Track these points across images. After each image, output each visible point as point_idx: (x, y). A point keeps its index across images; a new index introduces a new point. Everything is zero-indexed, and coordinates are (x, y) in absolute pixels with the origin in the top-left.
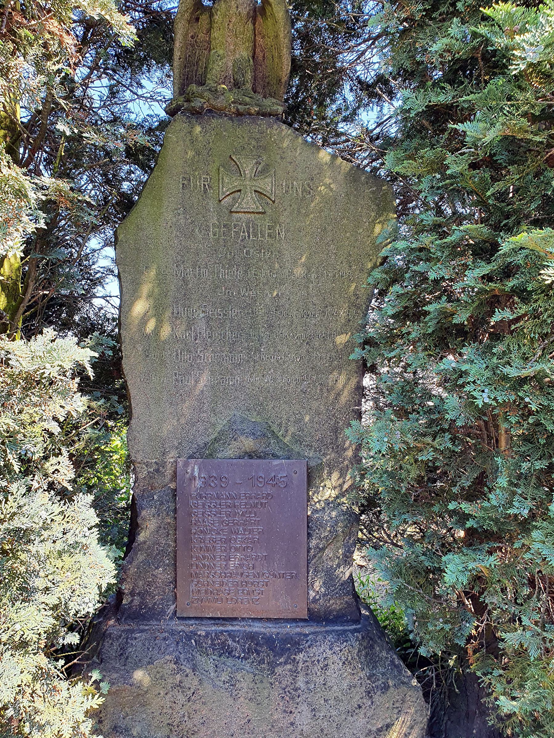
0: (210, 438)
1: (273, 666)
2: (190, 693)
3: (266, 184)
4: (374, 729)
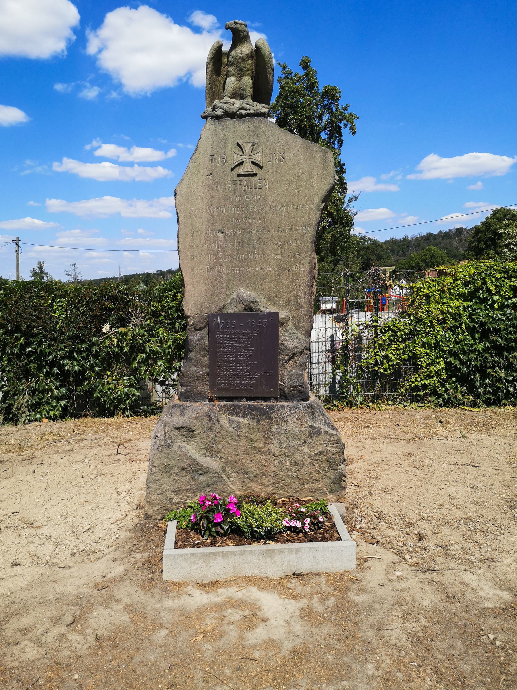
1: (259, 421)
2: (216, 433)
3: (258, 158)
4: (313, 454)
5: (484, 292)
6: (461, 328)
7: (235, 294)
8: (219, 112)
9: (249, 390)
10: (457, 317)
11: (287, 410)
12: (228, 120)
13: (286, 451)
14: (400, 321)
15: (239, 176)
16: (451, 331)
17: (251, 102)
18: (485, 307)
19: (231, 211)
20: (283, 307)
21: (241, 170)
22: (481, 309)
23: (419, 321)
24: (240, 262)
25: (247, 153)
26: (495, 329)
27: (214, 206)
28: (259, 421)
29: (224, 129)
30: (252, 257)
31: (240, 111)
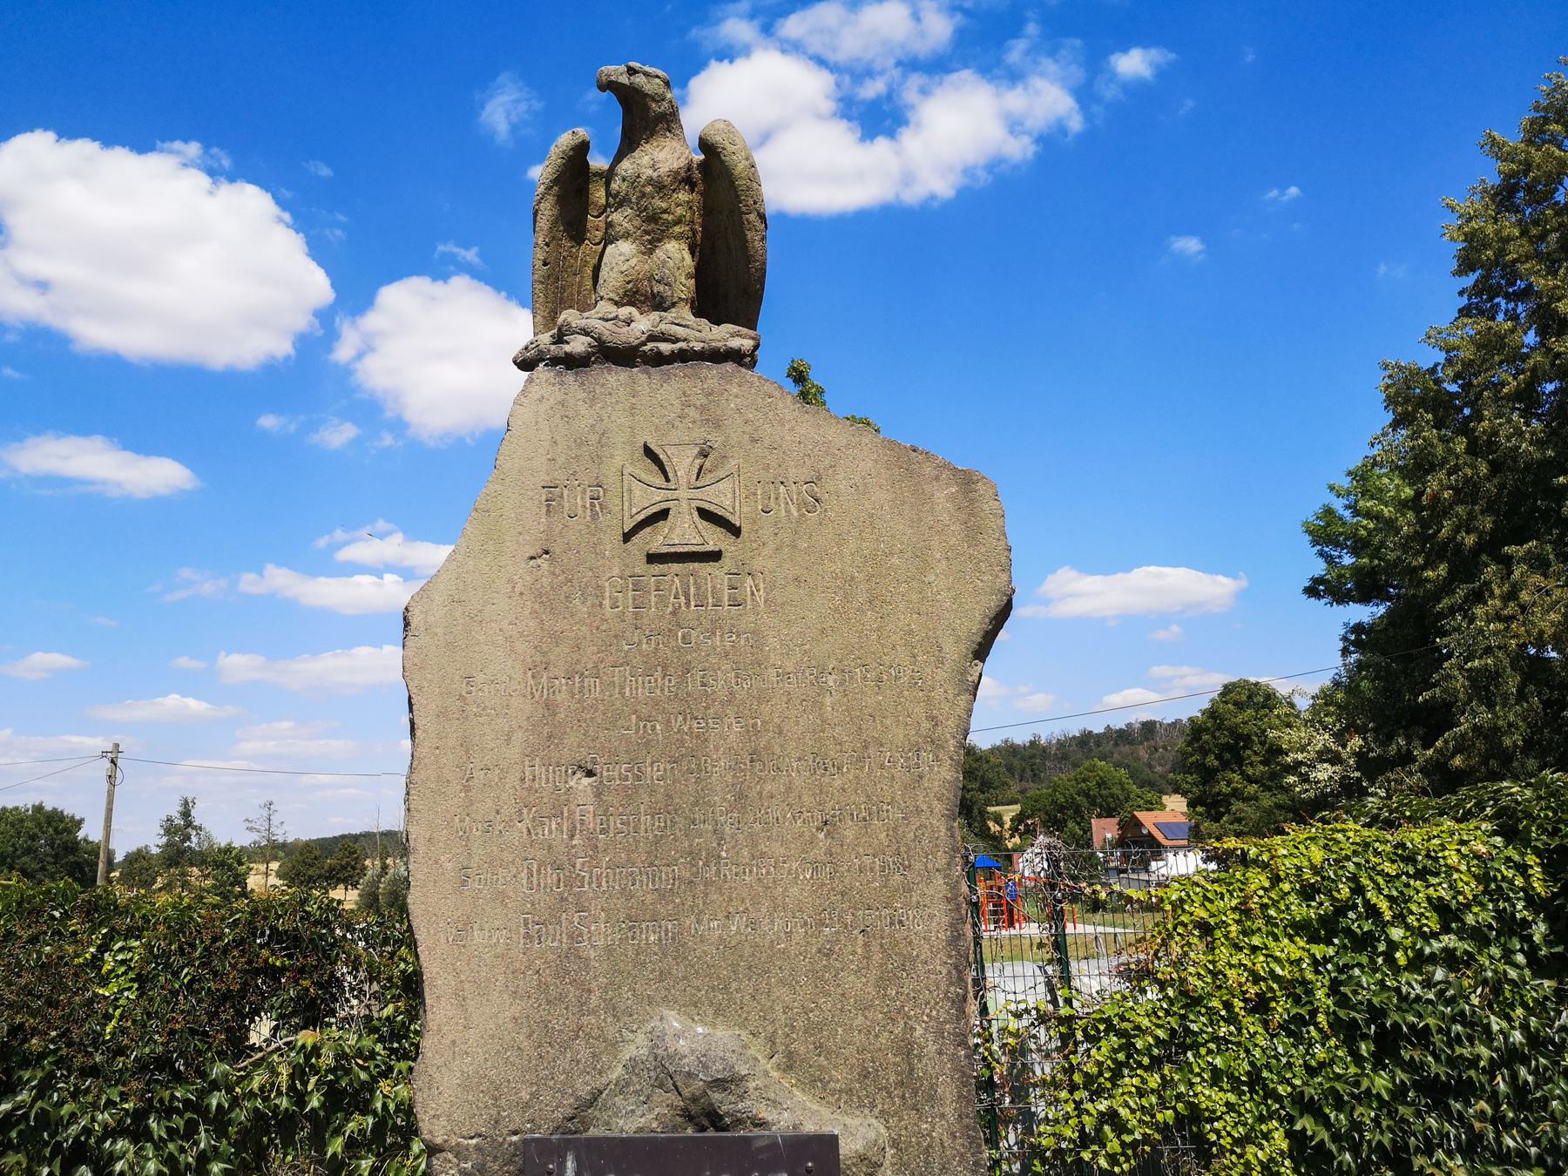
0: (604, 1080)
3: (721, 498)
5: (1359, 917)
6: (1316, 1025)
7: (641, 1039)
8: (578, 345)
10: (1298, 990)
12: (610, 370)
14: (1136, 1002)
15: (653, 558)
16: (1290, 1034)
17: (690, 318)
18: (1372, 961)
19: (622, 688)
20: (847, 1098)
21: (656, 539)
22: (1359, 965)
23: (1193, 1001)
24: (662, 895)
25: (683, 482)
26: (1412, 1027)
27: (554, 672)
29: (593, 401)
30: (710, 873)
31: (650, 345)
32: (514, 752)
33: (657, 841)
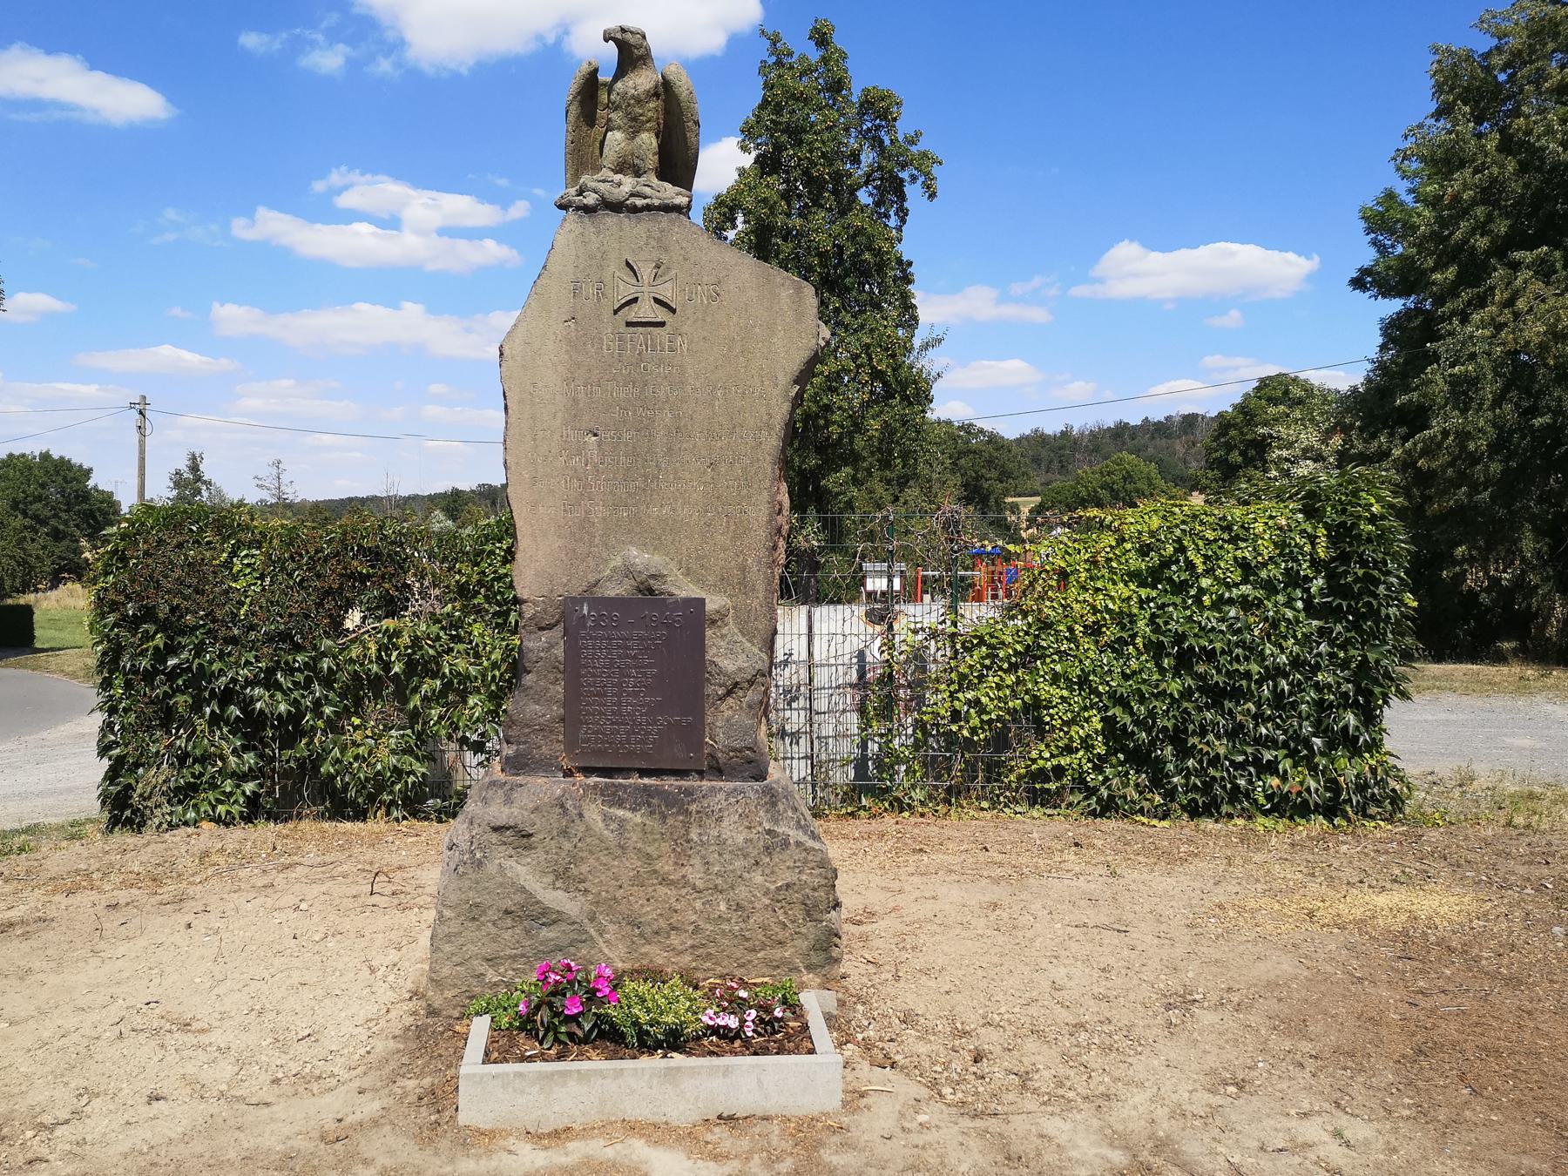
1: (664, 817)
3: (666, 292)
4: (773, 887)
5: (1180, 569)
6: (1134, 645)
7: (619, 558)
8: (590, 199)
9: (644, 755)
10: (1123, 619)
11: (721, 796)
13: (719, 881)
14: (1006, 625)
15: (629, 324)
16: (1114, 650)
17: (655, 181)
18: (1184, 601)
21: (632, 314)
22: (1175, 605)
23: (1046, 625)
26: (1203, 648)
28: (664, 817)
30: (654, 486)
31: (632, 200)
32: (558, 422)
33: (628, 469)
